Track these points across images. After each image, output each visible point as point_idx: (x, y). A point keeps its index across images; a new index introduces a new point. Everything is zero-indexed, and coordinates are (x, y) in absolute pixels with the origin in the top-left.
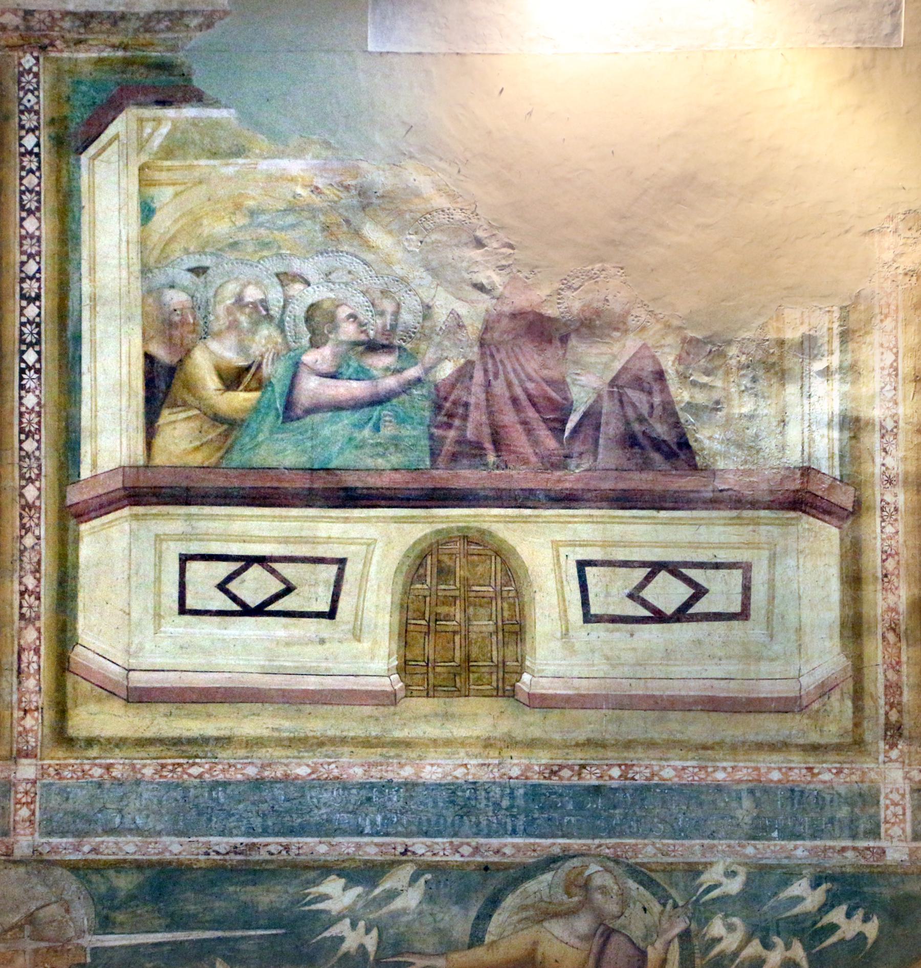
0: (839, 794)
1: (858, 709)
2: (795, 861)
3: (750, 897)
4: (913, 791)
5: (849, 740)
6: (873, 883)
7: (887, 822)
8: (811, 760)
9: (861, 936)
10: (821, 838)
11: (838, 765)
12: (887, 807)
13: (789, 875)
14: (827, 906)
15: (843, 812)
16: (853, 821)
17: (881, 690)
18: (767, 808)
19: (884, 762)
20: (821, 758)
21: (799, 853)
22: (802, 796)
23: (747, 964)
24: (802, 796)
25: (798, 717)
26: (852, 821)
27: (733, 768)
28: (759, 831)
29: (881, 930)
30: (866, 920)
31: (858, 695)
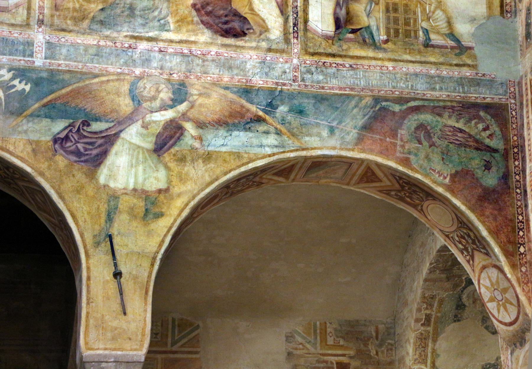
1: (29, 14)
2: (3, 63)
4: (46, 43)
5: (25, 23)
6: (30, 72)
8: (11, 29)
9: (24, 90)
12: (36, 47)
14: (13, 79)
15: (21, 48)
16: (24, 51)
17: (37, 7)
20: (14, 29)
25: (7, 14)
29: (31, 88)
30: (26, 84)
31: (29, 8)
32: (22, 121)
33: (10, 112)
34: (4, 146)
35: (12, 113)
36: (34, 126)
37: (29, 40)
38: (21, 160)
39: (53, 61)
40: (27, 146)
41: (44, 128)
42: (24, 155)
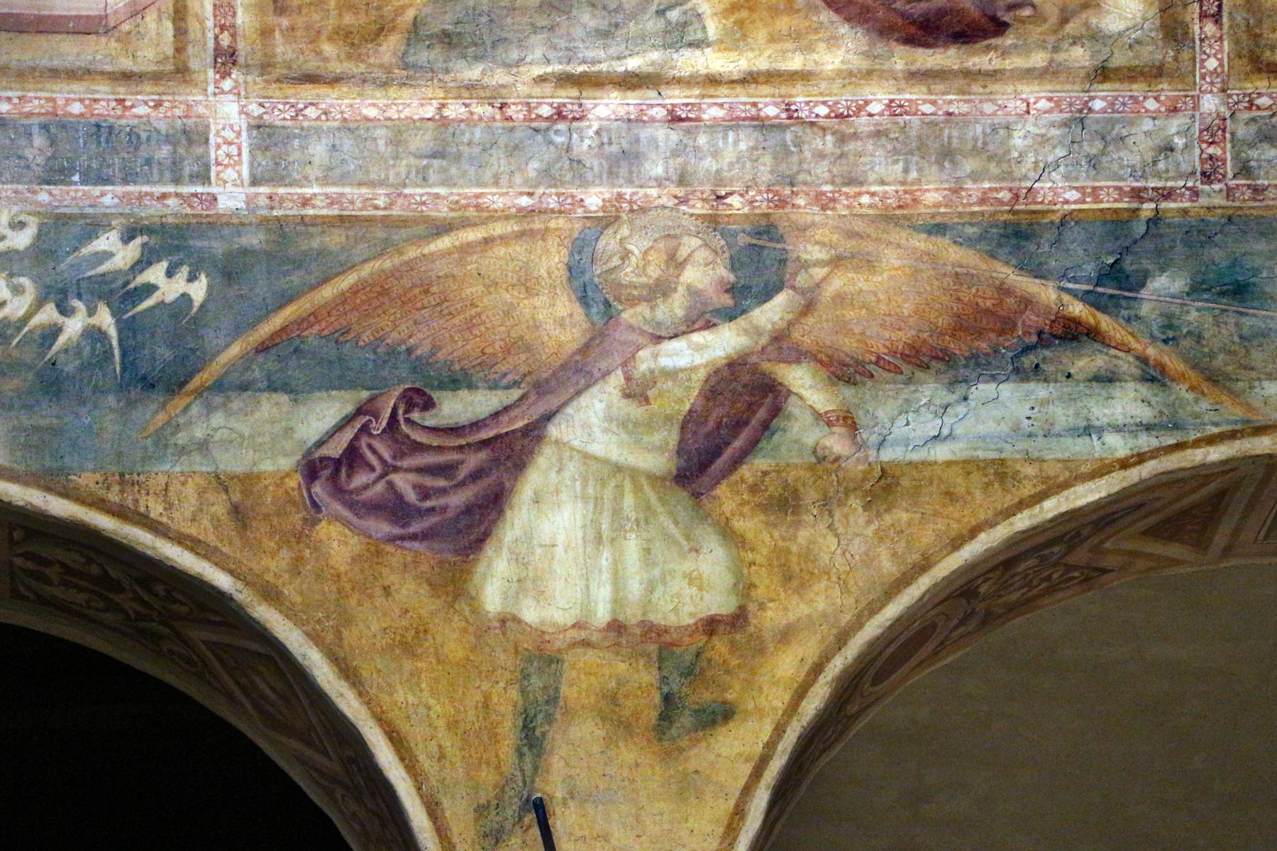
0: (159, 132)
2: (103, 210)
3: (42, 255)
4: (250, 127)
5: (169, 67)
6: (202, 236)
7: (218, 164)
8: (122, 91)
9: (185, 297)
10: (135, 183)
11: (156, 97)
12: (218, 147)
13: (95, 226)
14: (142, 264)
15: (164, 152)
18: (64, 147)
19: (215, 94)
21: (107, 200)
22: (110, 134)
23: (39, 332)
24: (110, 134)
25: (103, 40)
26: (174, 163)
27: (20, 98)
28: (55, 174)
29: (210, 289)
30: (192, 278)
32: (186, 409)
33: (144, 378)
34: (129, 503)
35: (149, 384)
36: (233, 423)
37: (190, 122)
38: (192, 550)
39: (281, 191)
40: (211, 496)
41: (267, 427)
42: (203, 530)
